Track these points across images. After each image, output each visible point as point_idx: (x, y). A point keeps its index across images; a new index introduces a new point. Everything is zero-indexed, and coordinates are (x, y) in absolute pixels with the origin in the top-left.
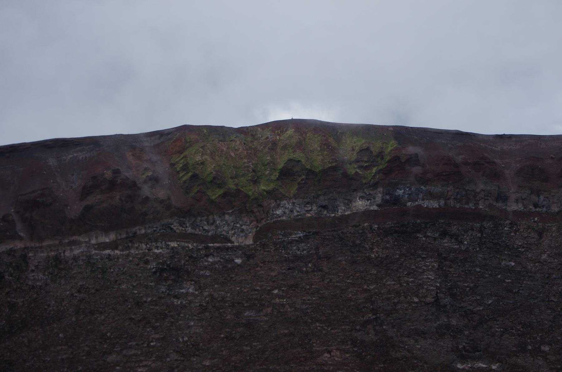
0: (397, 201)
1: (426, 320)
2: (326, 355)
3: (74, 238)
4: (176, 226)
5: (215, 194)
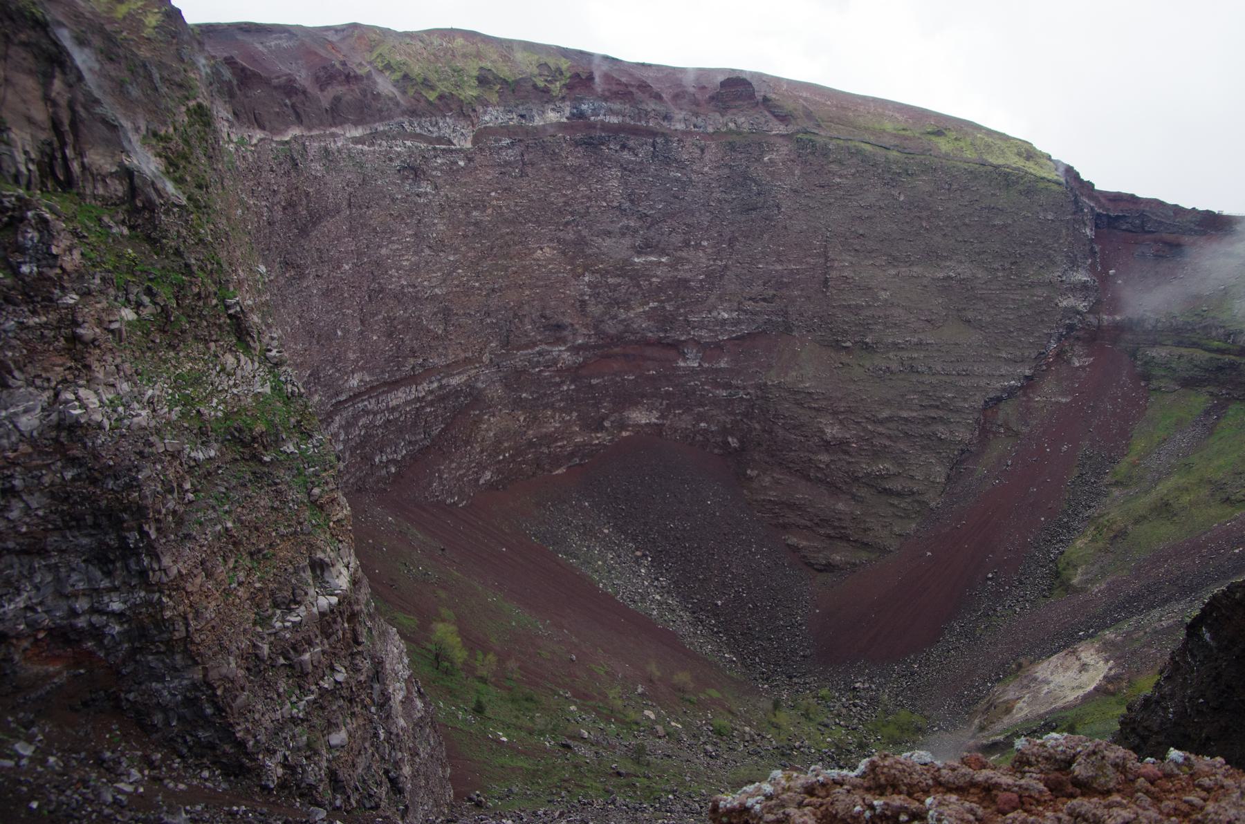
0: (581, 115)
1: (612, 222)
2: (539, 251)
3: (333, 130)
4: (406, 125)
5: (432, 96)
